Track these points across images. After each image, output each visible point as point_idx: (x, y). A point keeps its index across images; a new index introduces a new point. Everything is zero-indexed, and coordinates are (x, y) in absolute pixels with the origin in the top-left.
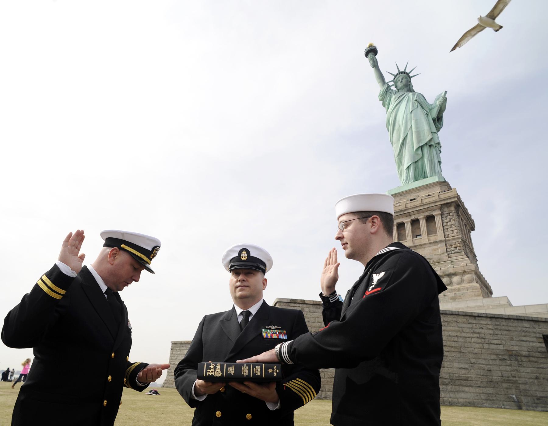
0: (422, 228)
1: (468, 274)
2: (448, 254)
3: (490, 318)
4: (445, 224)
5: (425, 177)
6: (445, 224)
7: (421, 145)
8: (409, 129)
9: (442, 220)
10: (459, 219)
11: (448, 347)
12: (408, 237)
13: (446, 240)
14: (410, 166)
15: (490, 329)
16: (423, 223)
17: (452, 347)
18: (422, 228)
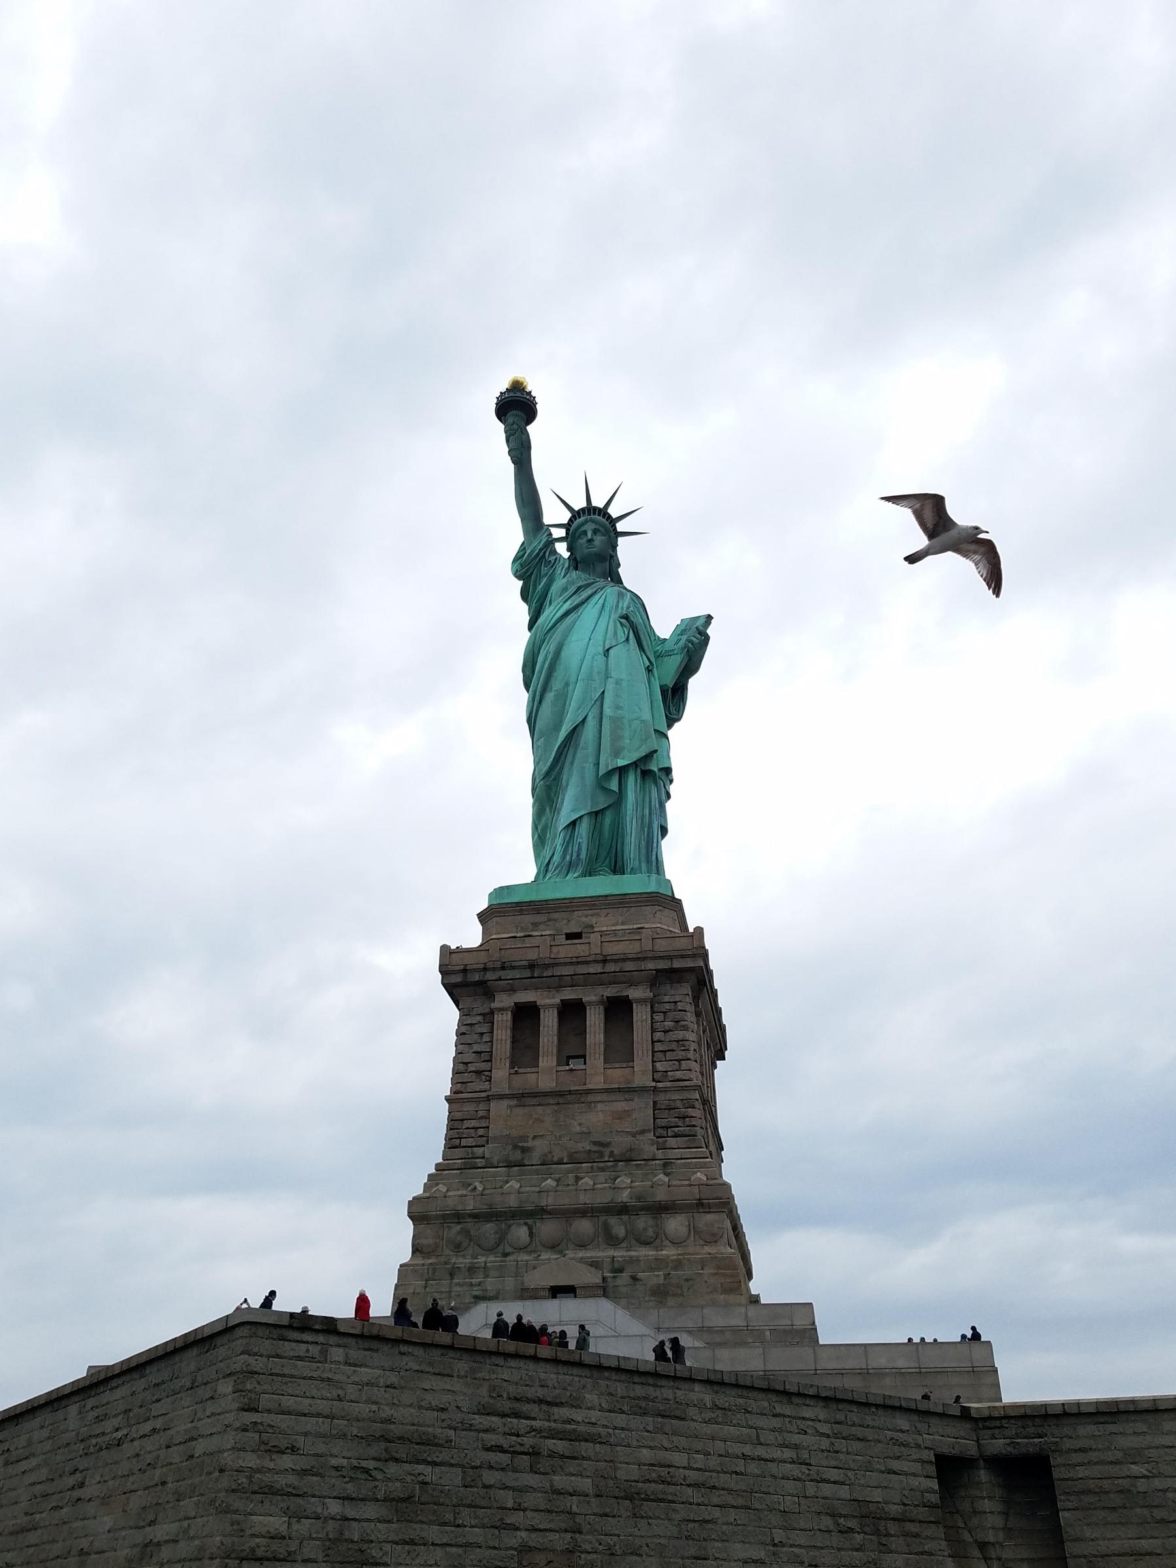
0: (592, 1035)
1: (710, 1212)
2: (658, 1137)
3: (826, 1399)
4: (658, 1036)
5: (618, 868)
6: (659, 1033)
7: (621, 763)
8: (593, 702)
10: (698, 1025)
11: (722, 1492)
12: (545, 1058)
13: (655, 1087)
14: (579, 821)
15: (822, 1435)
16: (595, 1019)
17: (730, 1491)
18: (592, 1035)
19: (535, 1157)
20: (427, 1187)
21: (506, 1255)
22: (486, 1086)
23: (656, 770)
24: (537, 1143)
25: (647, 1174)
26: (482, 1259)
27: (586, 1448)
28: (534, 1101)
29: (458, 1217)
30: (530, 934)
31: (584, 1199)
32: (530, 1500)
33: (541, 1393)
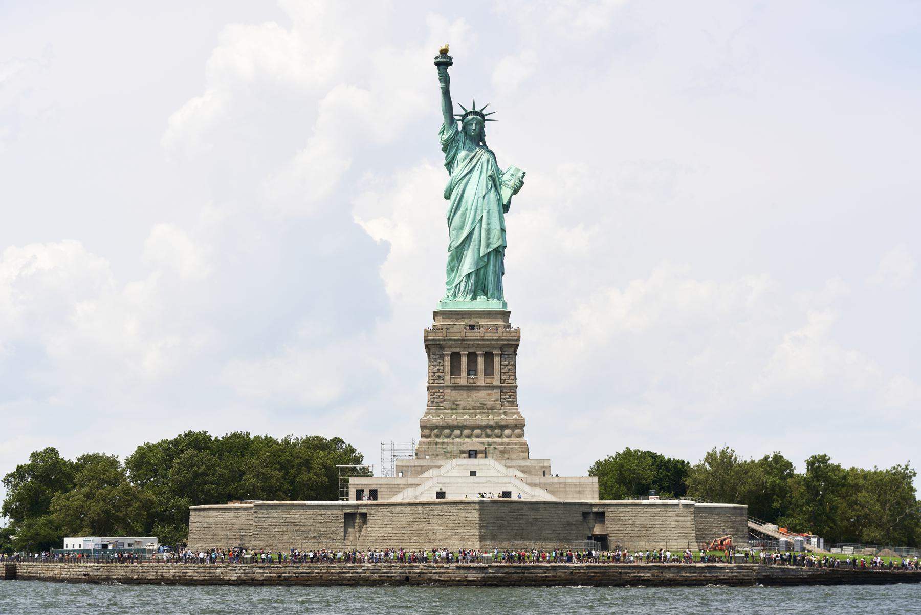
4: (502, 367)
7: (489, 250)
9: (501, 362)
16: (480, 360)
19: (461, 407)
20: (425, 416)
21: (453, 439)
22: (442, 382)
23: (501, 251)
24: (462, 402)
25: (498, 415)
26: (446, 440)
27: (524, 516)
28: (460, 388)
29: (437, 427)
30: (455, 323)
31: (479, 423)
32: (517, 525)
33: (517, 508)
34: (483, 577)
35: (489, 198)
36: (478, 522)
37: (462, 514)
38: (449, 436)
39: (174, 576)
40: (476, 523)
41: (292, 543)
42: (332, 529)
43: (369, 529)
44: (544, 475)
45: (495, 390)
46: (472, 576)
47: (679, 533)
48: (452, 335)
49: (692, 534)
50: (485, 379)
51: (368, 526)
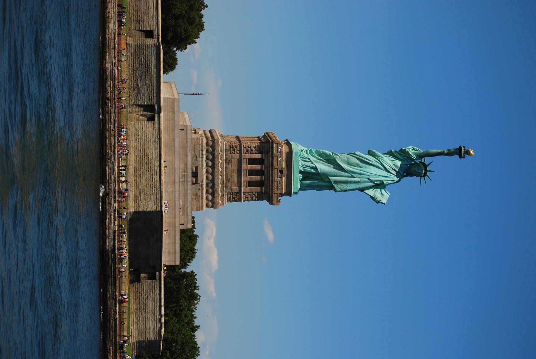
9: (257, 192)
21: (205, 161)
26: (205, 156)
29: (214, 150)
31: (216, 178)
34: (109, 250)
35: (368, 182)
36: (148, 210)
37: (153, 197)
38: (207, 158)
39: (109, 12)
40: (147, 209)
41: (134, 70)
42: (143, 97)
43: (143, 123)
44: (180, 224)
45: (238, 188)
46: (109, 242)
47: (142, 330)
48: (276, 160)
49: (141, 339)
50: (245, 160)
51: (145, 122)
